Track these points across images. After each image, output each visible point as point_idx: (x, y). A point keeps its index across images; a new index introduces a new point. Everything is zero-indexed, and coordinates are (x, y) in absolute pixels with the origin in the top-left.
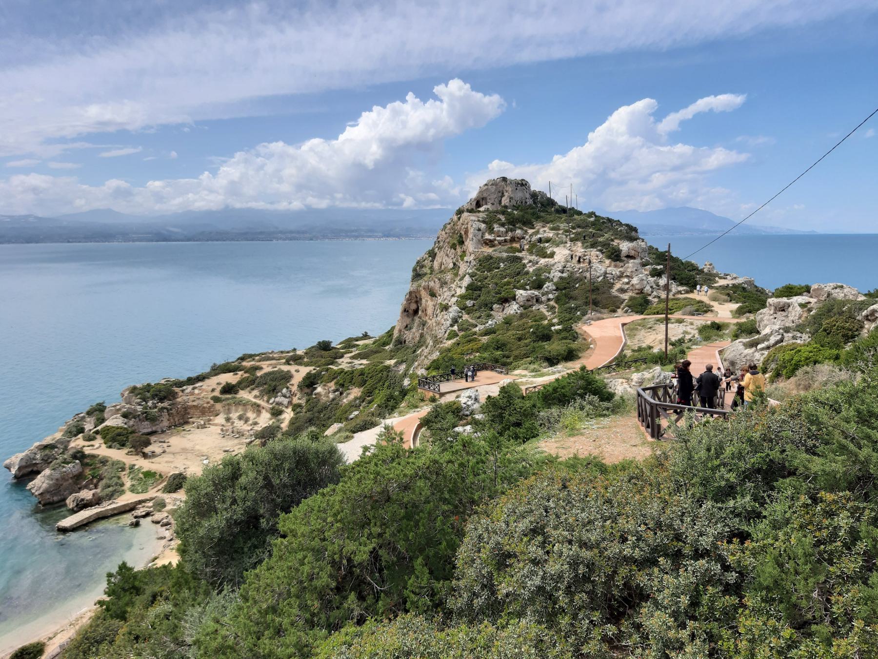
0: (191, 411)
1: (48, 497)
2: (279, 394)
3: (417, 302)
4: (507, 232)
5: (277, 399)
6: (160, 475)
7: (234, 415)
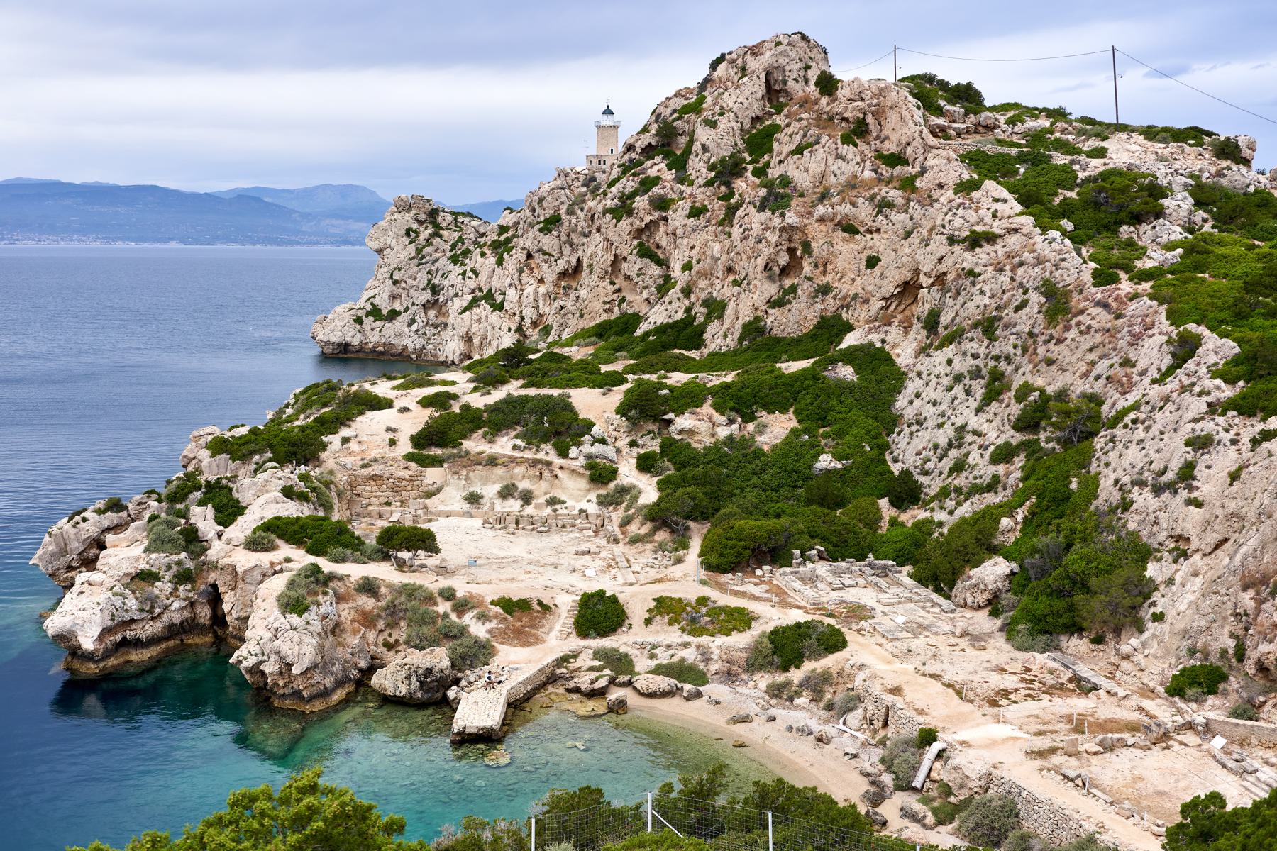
0: (365, 490)
1: (317, 678)
2: (587, 437)
3: (791, 251)
4: (966, 114)
5: (587, 449)
6: (540, 603)
7: (490, 491)
